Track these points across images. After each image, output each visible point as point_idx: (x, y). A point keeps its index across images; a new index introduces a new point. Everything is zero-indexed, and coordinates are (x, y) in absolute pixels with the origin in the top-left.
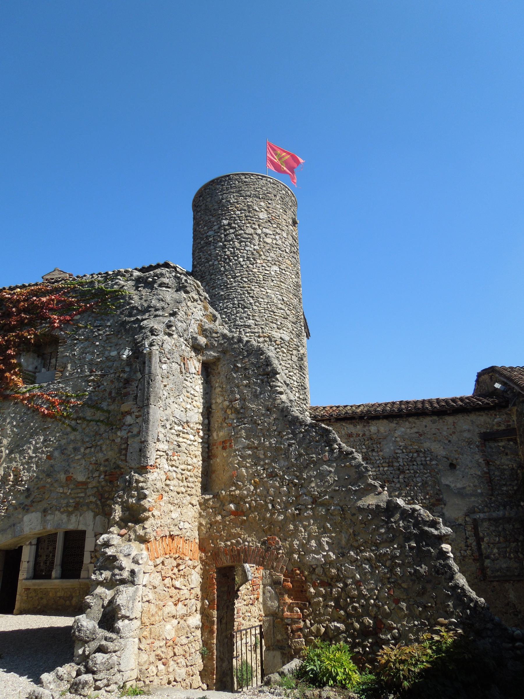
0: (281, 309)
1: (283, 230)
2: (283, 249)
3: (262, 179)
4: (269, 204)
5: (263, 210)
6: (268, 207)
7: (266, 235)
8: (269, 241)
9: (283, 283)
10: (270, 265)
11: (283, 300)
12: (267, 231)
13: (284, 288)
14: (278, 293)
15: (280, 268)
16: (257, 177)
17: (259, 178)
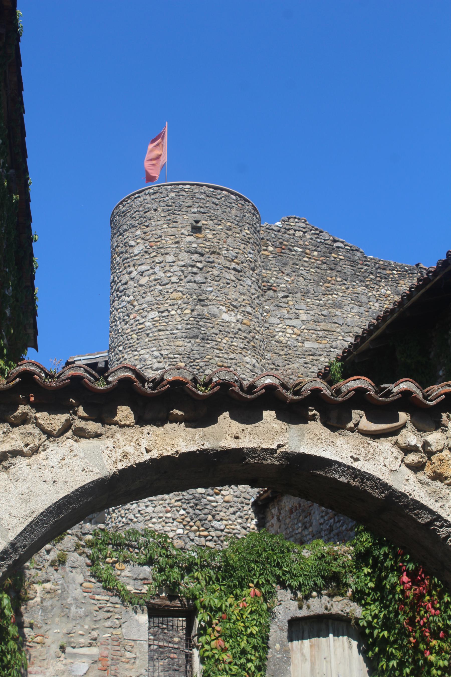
0: (157, 369)
1: (167, 254)
2: (166, 280)
3: (139, 197)
4: (147, 226)
5: (139, 241)
6: (145, 233)
7: (142, 274)
8: (144, 280)
9: (163, 331)
10: (145, 313)
11: (162, 355)
12: (143, 268)
13: (162, 337)
14: (154, 349)
15: (159, 312)
16: (133, 197)
17: (136, 198)
